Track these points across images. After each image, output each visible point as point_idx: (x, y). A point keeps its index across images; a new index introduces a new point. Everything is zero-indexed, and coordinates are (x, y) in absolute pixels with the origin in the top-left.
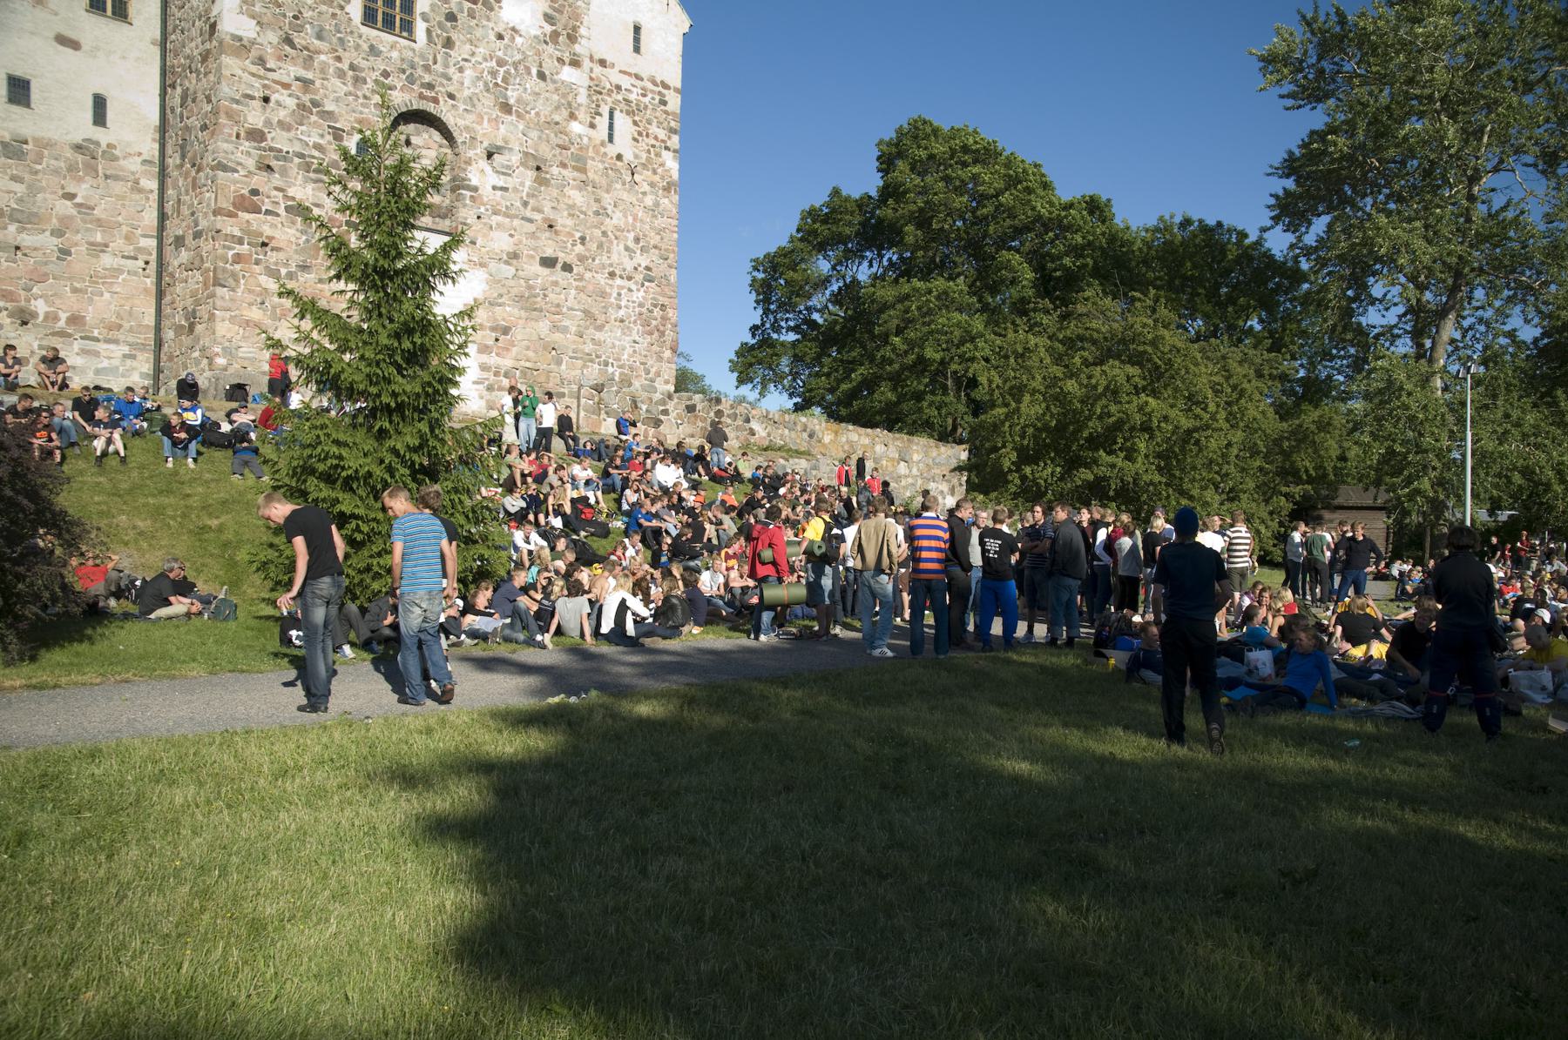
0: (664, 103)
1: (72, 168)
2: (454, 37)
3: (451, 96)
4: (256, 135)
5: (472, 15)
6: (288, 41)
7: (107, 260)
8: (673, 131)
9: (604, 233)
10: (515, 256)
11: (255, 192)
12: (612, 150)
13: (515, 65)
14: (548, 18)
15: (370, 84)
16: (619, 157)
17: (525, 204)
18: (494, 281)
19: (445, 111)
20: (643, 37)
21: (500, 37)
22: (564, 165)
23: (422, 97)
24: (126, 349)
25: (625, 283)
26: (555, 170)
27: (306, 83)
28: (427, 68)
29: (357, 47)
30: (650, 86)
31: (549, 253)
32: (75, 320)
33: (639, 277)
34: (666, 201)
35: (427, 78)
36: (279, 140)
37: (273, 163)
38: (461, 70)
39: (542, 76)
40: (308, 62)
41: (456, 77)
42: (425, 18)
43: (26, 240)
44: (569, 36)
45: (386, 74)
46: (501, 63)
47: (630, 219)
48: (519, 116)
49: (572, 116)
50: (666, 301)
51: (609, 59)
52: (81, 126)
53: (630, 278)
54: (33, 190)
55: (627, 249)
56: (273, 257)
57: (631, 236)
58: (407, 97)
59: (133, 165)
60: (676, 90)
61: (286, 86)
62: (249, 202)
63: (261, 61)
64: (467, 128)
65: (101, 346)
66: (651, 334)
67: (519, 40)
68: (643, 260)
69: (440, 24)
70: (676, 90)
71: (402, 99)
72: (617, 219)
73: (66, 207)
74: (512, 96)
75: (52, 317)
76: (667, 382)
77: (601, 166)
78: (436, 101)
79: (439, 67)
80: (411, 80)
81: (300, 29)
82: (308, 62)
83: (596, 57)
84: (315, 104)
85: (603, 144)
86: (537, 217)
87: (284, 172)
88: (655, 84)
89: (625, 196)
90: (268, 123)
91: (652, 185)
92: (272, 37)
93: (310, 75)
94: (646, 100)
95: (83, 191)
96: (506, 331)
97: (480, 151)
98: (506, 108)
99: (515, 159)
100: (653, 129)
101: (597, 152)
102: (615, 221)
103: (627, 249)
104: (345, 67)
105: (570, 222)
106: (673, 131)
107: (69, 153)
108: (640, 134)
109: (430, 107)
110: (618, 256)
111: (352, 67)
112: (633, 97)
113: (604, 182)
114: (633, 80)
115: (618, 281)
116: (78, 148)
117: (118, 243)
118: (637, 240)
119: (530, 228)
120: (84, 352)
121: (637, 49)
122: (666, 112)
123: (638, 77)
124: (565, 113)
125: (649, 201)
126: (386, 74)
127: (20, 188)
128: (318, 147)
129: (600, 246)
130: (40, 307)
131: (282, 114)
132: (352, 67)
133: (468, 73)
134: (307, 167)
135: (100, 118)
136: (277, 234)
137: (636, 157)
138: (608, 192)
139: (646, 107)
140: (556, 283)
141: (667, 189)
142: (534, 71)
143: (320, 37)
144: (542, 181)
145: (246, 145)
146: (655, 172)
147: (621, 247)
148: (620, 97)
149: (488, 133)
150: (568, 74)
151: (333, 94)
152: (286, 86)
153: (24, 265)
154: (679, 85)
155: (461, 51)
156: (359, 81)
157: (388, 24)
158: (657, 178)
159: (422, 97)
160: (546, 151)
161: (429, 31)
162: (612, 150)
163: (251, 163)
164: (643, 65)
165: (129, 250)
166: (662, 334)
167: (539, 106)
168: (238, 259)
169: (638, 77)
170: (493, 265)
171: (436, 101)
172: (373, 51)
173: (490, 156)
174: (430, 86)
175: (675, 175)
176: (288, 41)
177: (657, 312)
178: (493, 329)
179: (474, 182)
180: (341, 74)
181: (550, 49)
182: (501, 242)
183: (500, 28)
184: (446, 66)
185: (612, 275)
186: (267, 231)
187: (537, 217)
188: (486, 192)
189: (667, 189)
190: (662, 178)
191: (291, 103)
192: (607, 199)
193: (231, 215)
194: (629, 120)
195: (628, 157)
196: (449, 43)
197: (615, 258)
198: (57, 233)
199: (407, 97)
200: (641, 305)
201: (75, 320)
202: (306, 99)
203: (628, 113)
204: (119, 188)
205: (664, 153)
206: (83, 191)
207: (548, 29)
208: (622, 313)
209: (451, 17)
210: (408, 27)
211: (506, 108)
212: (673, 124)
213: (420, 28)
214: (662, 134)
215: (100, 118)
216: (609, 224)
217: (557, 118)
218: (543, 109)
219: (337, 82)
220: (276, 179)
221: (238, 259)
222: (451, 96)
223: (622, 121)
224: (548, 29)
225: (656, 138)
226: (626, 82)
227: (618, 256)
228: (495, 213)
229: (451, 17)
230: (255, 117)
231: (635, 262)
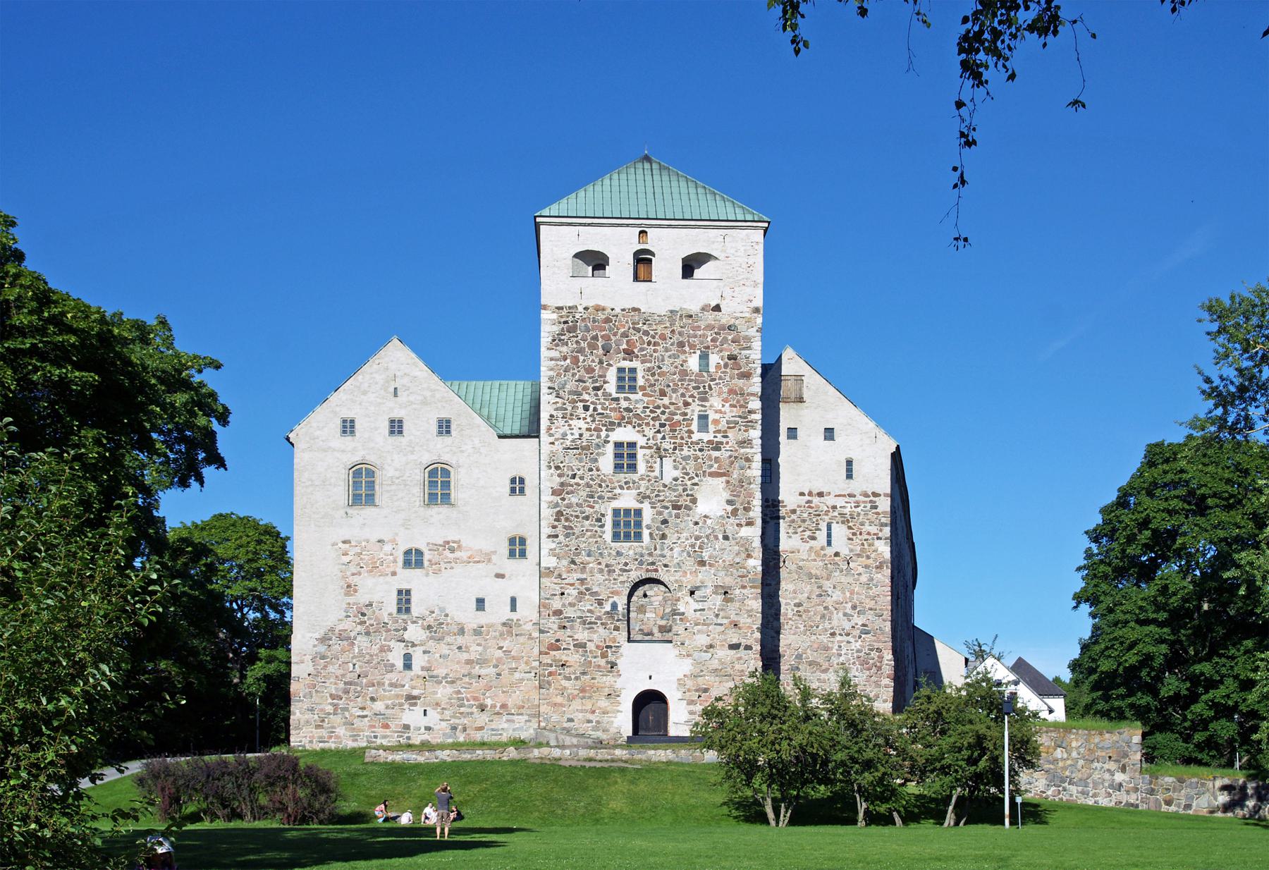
0: (876, 507)
1: (502, 634)
2: (666, 531)
3: (666, 566)
4: (558, 613)
5: (677, 516)
6: (573, 562)
7: (517, 675)
8: (883, 525)
9: (826, 608)
10: (711, 646)
11: (558, 641)
12: (830, 551)
13: (707, 537)
14: (729, 502)
15: (617, 572)
16: (837, 554)
17: (717, 616)
18: (697, 663)
19: (662, 575)
20: (854, 467)
21: (696, 523)
22: (744, 587)
23: (648, 570)
24: (526, 718)
25: (845, 638)
26: (737, 592)
27: (582, 581)
28: (650, 554)
29: (610, 554)
30: (862, 498)
31: (735, 641)
32: (504, 706)
33: (857, 633)
34: (879, 576)
35: (651, 560)
36: (570, 612)
37: (567, 624)
38: (672, 549)
39: (726, 538)
40: (583, 570)
41: (666, 552)
42: (648, 527)
43: (483, 672)
44: (745, 509)
45: (626, 564)
46: (697, 538)
47: (848, 594)
48: (710, 565)
49: (749, 556)
50: (881, 645)
51: (825, 490)
52: (506, 614)
53: (848, 635)
54: (485, 648)
55: (845, 614)
56: (567, 670)
57: (850, 605)
58: (639, 573)
59: (529, 627)
60: (886, 495)
61: (572, 585)
62: (555, 646)
63: (560, 576)
64: (676, 581)
65: (515, 717)
66: (869, 669)
67: (709, 522)
68: (859, 621)
69: (658, 529)
70: (886, 495)
71: (635, 575)
72: (837, 595)
73: (499, 653)
74: (706, 556)
75: (494, 706)
76: (885, 701)
77: (821, 564)
78: (656, 571)
79: (658, 552)
80: (641, 563)
81: (578, 554)
82: (583, 570)
83: (815, 492)
84: (587, 589)
85: (822, 548)
86: (725, 621)
87: (572, 628)
88: (866, 495)
89: (843, 579)
90: (564, 605)
91: (867, 567)
92: (565, 562)
93: (584, 576)
94: (859, 509)
95: (506, 644)
96: (706, 690)
97: (685, 592)
98: (702, 563)
99: (709, 591)
100: (867, 528)
101: (817, 554)
102: (835, 598)
103: (845, 614)
104: (603, 566)
105: (749, 620)
106: (883, 525)
107: (500, 628)
108: (854, 534)
109: (653, 575)
110: (838, 620)
111: (607, 566)
112: (847, 511)
113: (825, 575)
114: (847, 499)
115: (838, 638)
116: (504, 624)
117: (523, 667)
118: (854, 607)
119: (722, 628)
120: (508, 721)
121: (849, 476)
122: (878, 514)
123: (850, 495)
124: (744, 556)
125: (864, 579)
126: (626, 564)
127: (480, 649)
128: (590, 611)
129: (823, 617)
130: (489, 702)
131: (571, 599)
132: (607, 566)
133: (677, 550)
134: (584, 623)
135: (513, 608)
136: (569, 659)
137: (851, 550)
138: (828, 579)
139: (859, 514)
140: (740, 658)
141: (880, 567)
142: (720, 537)
143: (589, 555)
144: (727, 600)
145: (553, 618)
146: (868, 557)
147: (841, 614)
148: (836, 514)
149: (689, 581)
150: (745, 532)
151: (598, 581)
152: (572, 585)
153: (483, 682)
154: (889, 491)
155: (672, 537)
156: (611, 572)
157: (627, 537)
158: (871, 561)
159: (648, 570)
160: (729, 581)
161: (651, 534)
162: (830, 551)
163: (555, 627)
164: (856, 486)
165: (527, 669)
166: (879, 668)
167: (725, 557)
168: (550, 674)
169: (850, 495)
170: (696, 655)
171: (656, 571)
172: (619, 554)
173: (692, 593)
174: (653, 564)
175: (888, 555)
176: (573, 562)
177: (874, 654)
178: (697, 690)
179: (682, 610)
180: (601, 571)
181: (732, 520)
182: (703, 640)
183: (696, 519)
184: (662, 549)
185: (833, 634)
186: (564, 658)
187: (725, 621)
188: (690, 614)
189: (880, 567)
190: (875, 560)
191: (575, 593)
192: (827, 585)
193: (547, 654)
194: (844, 527)
195: (844, 551)
196: (664, 537)
197: (835, 623)
198: (496, 666)
199: (639, 573)
200: (858, 651)
201: (504, 706)
202: (582, 589)
203: (843, 522)
204: (521, 639)
205: (877, 543)
206: (506, 644)
207: (730, 508)
208: (842, 659)
209: (665, 522)
210: (638, 536)
211: (702, 563)
212: (883, 520)
213: (646, 533)
214: (873, 529)
215: (513, 608)
216: (829, 602)
217: (737, 560)
218: (728, 558)
219: (599, 576)
220: (568, 632)
221: (550, 674)
222: (666, 566)
223: (839, 531)
224: (730, 508)
225: (869, 534)
226: (840, 502)
227: (838, 620)
228: (696, 624)
229: (665, 522)
230: (557, 604)
231: (852, 623)
